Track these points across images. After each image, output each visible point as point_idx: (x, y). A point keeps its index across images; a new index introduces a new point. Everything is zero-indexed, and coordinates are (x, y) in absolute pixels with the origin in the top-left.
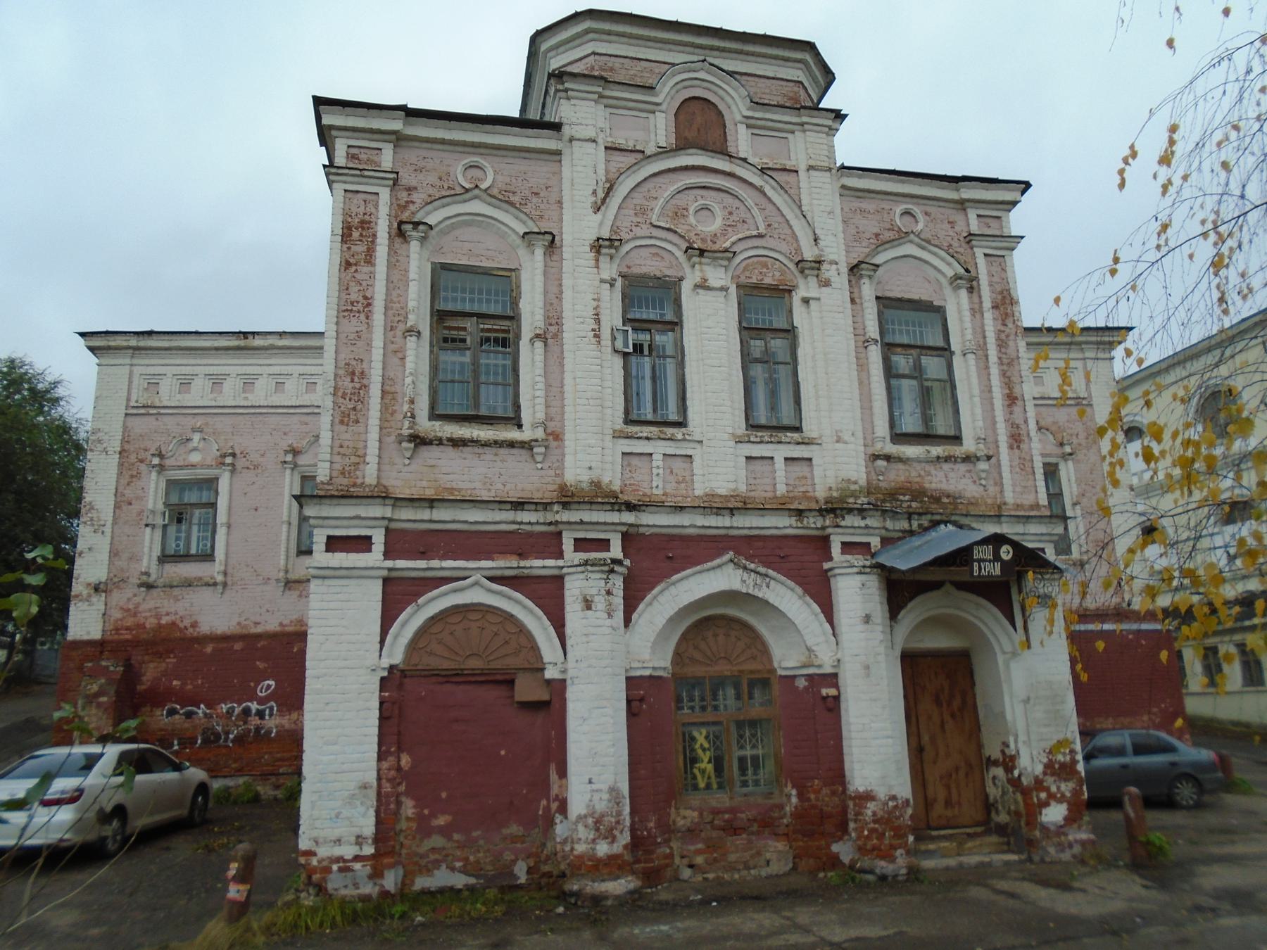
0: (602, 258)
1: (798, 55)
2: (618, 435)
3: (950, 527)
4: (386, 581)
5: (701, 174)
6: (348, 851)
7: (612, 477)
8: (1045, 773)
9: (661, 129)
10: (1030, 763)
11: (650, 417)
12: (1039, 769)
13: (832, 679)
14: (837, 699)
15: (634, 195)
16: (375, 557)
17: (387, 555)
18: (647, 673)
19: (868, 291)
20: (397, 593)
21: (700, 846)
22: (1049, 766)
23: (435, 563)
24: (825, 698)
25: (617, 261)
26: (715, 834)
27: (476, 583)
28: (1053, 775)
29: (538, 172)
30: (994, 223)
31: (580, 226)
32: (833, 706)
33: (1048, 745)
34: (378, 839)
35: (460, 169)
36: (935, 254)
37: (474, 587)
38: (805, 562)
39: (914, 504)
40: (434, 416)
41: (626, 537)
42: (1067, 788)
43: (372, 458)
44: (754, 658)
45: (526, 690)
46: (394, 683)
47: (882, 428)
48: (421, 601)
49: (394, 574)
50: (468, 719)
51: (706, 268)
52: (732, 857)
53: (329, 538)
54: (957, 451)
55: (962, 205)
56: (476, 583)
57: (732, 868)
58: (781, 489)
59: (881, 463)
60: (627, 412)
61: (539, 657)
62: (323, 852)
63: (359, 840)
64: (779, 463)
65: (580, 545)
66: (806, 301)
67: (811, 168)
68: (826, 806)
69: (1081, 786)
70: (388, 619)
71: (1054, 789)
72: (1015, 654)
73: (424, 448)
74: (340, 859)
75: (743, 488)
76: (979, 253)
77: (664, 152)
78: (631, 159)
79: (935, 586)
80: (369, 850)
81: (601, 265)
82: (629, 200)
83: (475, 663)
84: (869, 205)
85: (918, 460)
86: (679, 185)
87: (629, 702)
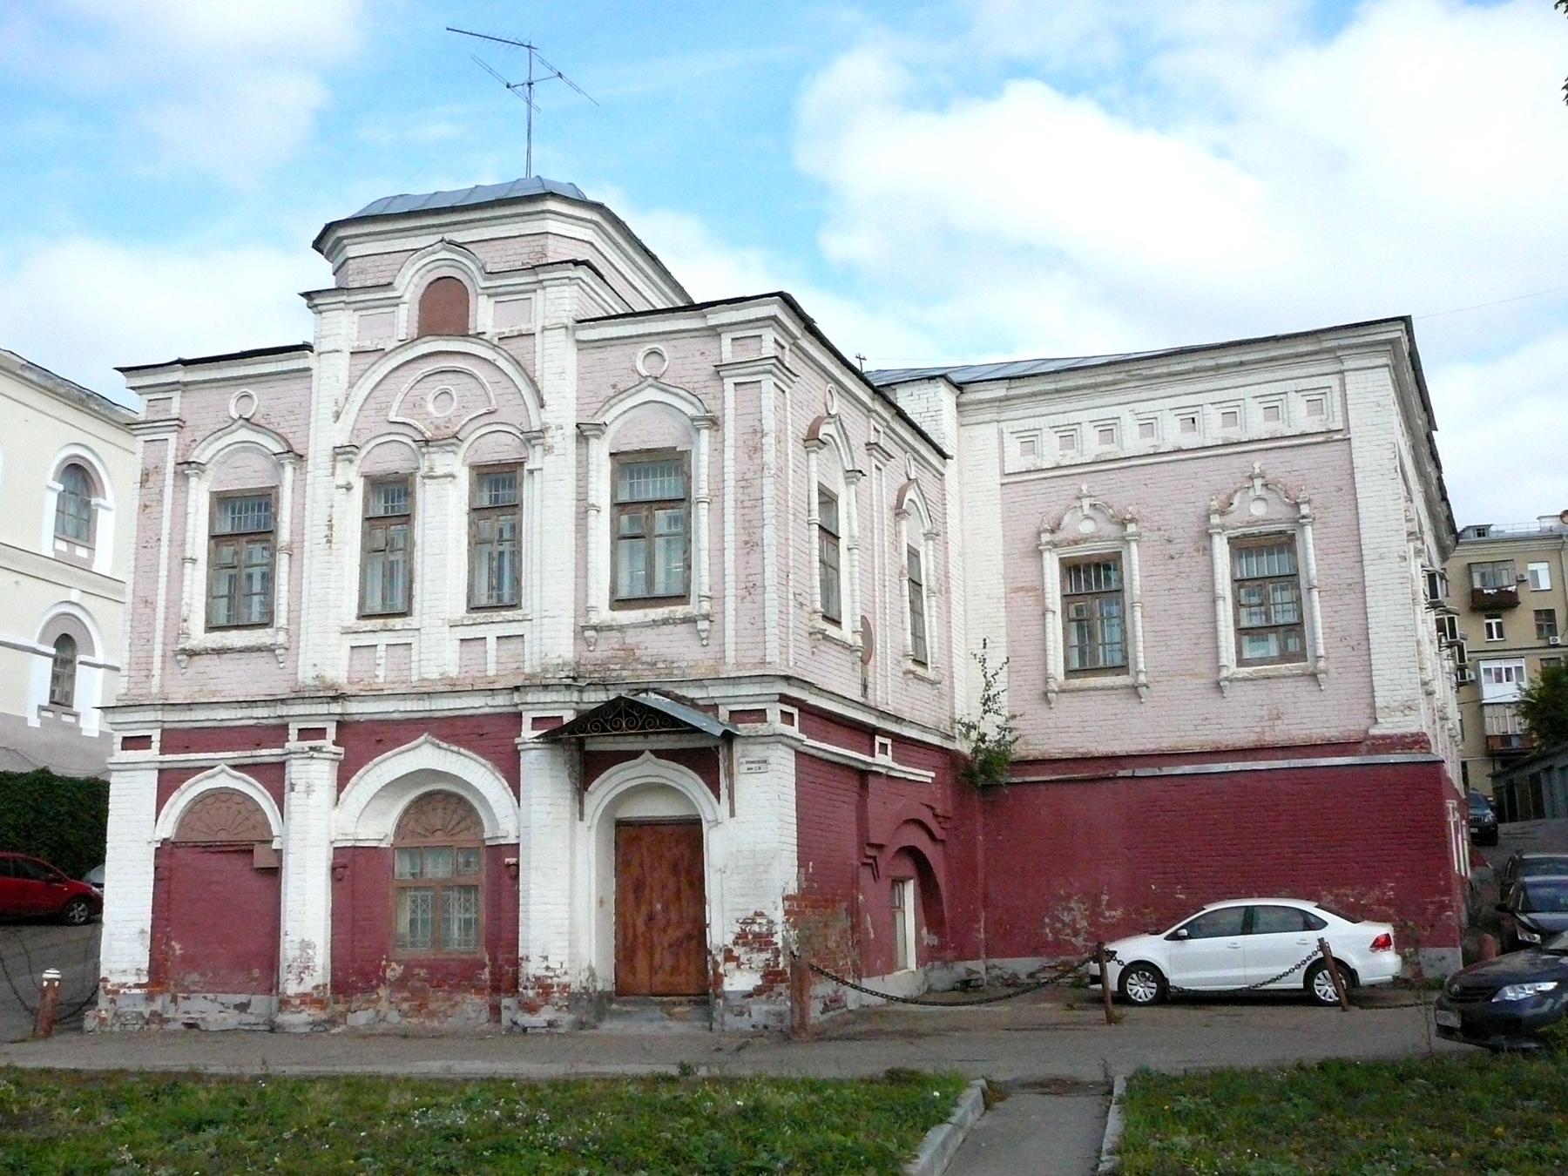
0: (339, 465)
1: (540, 207)
2: (347, 631)
3: (653, 696)
4: (161, 771)
5: (440, 358)
6: (131, 980)
7: (338, 672)
8: (735, 943)
9: (405, 319)
10: (720, 933)
11: (378, 610)
12: (729, 940)
13: (515, 849)
14: (517, 865)
15: (376, 393)
16: (153, 753)
17: (163, 751)
18: (349, 844)
19: (600, 451)
20: (169, 782)
21: (406, 994)
22: (741, 938)
23: (193, 756)
24: (509, 865)
25: (357, 462)
26: (418, 984)
27: (223, 771)
28: (744, 945)
29: (288, 392)
30: (752, 343)
31: (323, 437)
32: (514, 872)
33: (742, 916)
34: (150, 972)
35: (233, 402)
36: (677, 395)
37: (220, 774)
38: (492, 737)
39: (625, 673)
40: (211, 628)
41: (341, 725)
42: (760, 958)
43: (157, 671)
44: (468, 829)
45: (261, 859)
46: (165, 851)
47: (600, 595)
48: (183, 786)
49: (165, 766)
50: (219, 882)
51: (435, 456)
52: (432, 1006)
53: (125, 738)
54: (679, 611)
55: (715, 332)
56: (223, 771)
57: (432, 1015)
58: (492, 671)
59: (590, 633)
60: (361, 605)
61: (270, 832)
62: (114, 980)
63: (138, 971)
64: (491, 643)
65: (304, 734)
66: (531, 472)
67: (544, 329)
68: (498, 967)
69: (777, 957)
70: (161, 802)
71: (743, 959)
72: (717, 823)
73: (196, 658)
74: (124, 985)
75: (453, 672)
76: (729, 384)
77: (405, 344)
78: (373, 358)
79: (634, 755)
80: (145, 980)
81: (338, 472)
82: (371, 400)
83: (223, 836)
84: (613, 355)
85: (635, 626)
86: (418, 374)
87: (334, 869)
